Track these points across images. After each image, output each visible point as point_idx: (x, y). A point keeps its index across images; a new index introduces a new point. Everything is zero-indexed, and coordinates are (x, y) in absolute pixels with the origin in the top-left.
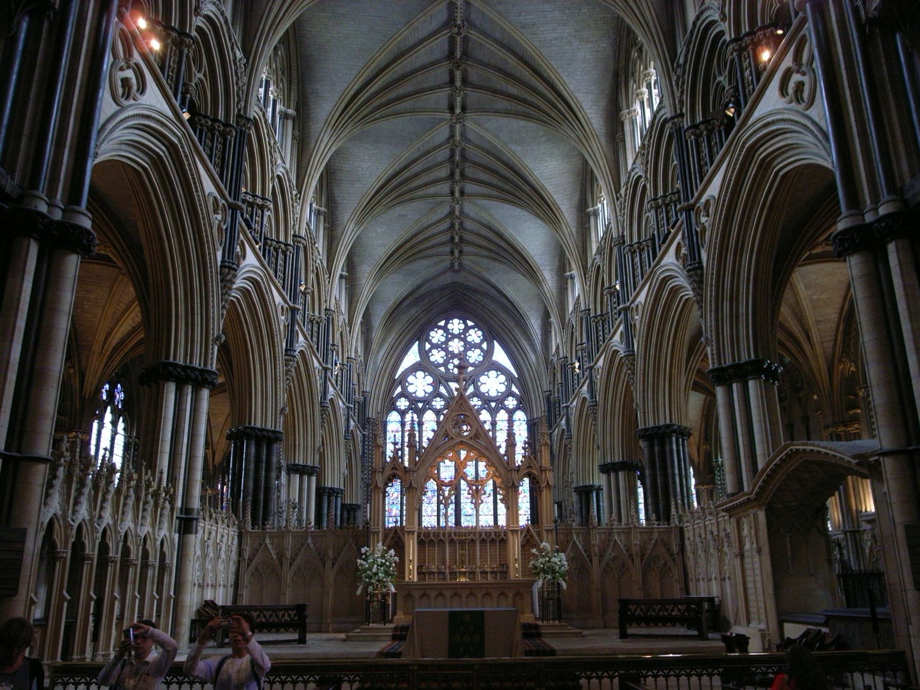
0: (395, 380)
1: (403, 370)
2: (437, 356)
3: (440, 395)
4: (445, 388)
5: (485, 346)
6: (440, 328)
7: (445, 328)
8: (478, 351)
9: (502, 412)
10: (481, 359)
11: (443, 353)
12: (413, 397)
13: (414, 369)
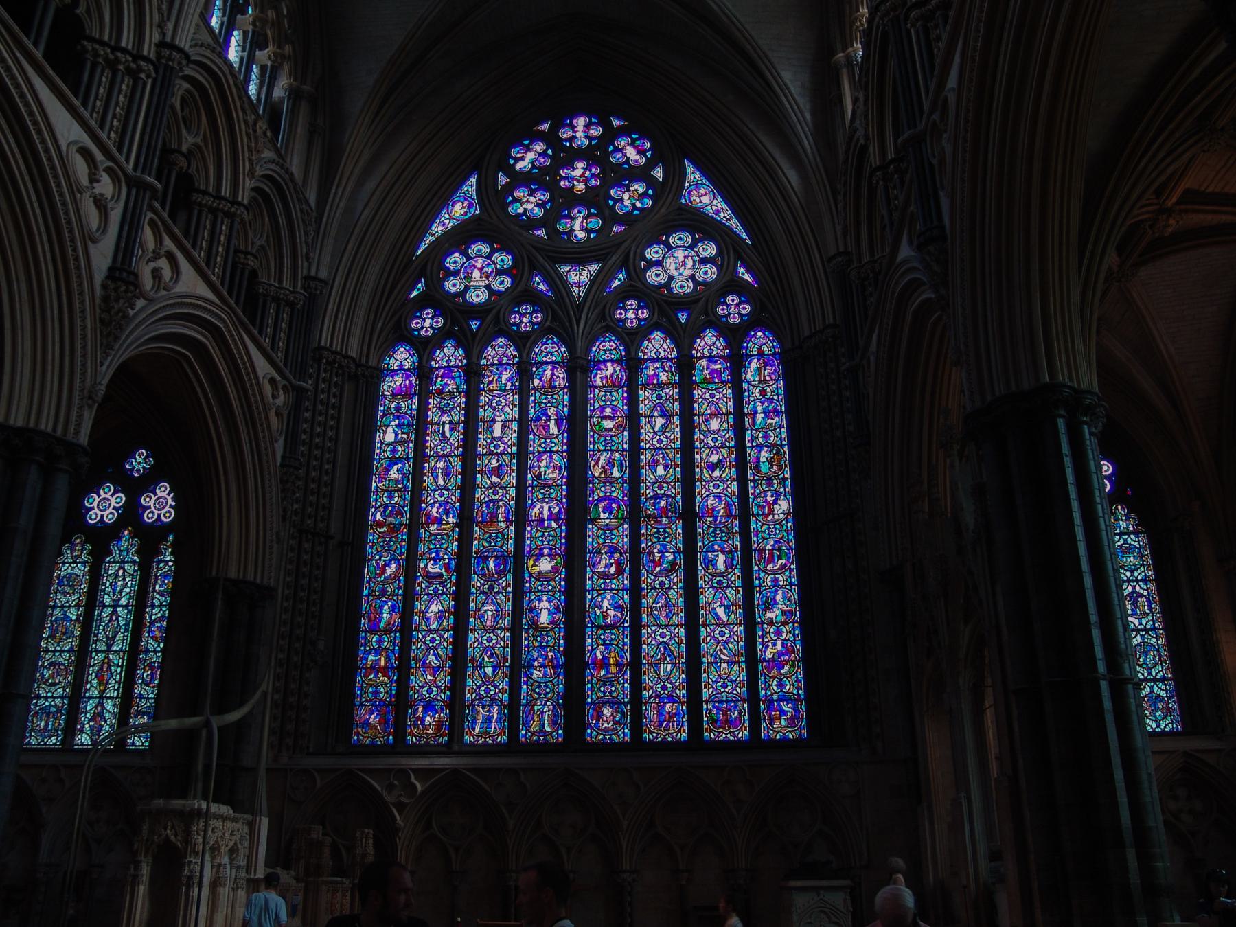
0: (410, 261)
1: (431, 239)
2: (528, 204)
3: (532, 297)
4: (547, 280)
5: (658, 173)
6: (540, 137)
7: (551, 139)
8: (639, 187)
9: (709, 334)
10: (648, 202)
11: (542, 196)
12: (458, 303)
13: (461, 237)
